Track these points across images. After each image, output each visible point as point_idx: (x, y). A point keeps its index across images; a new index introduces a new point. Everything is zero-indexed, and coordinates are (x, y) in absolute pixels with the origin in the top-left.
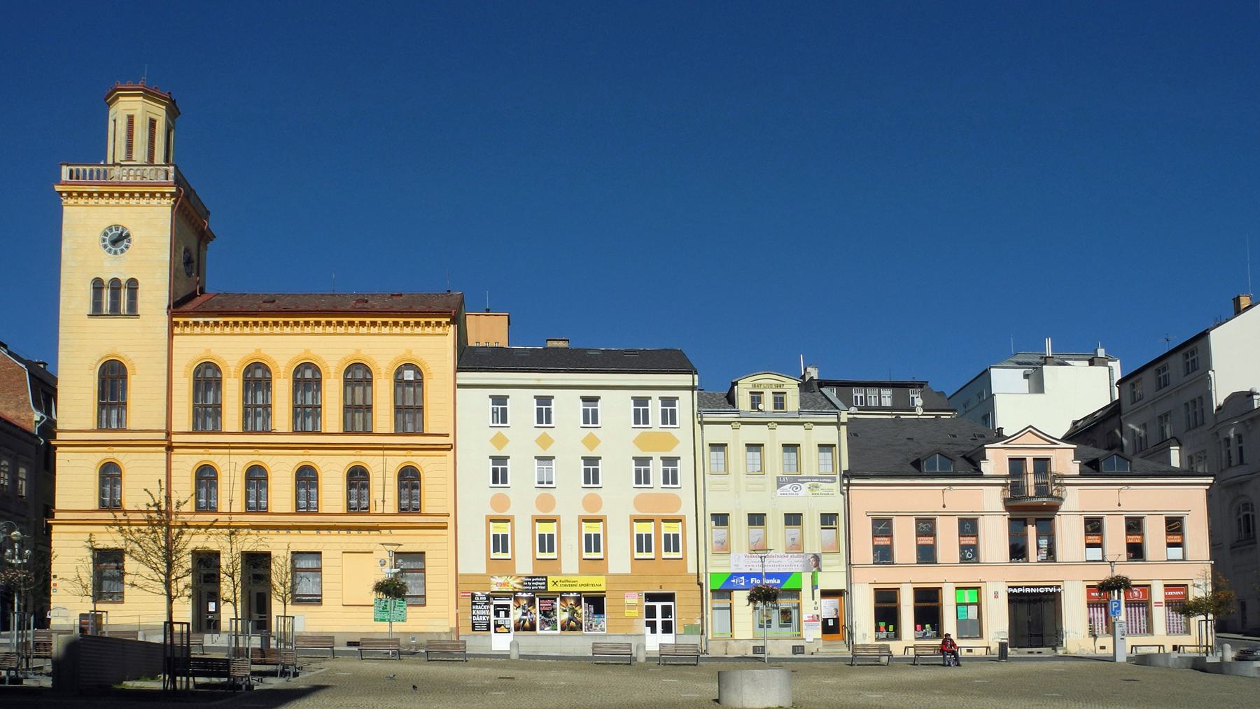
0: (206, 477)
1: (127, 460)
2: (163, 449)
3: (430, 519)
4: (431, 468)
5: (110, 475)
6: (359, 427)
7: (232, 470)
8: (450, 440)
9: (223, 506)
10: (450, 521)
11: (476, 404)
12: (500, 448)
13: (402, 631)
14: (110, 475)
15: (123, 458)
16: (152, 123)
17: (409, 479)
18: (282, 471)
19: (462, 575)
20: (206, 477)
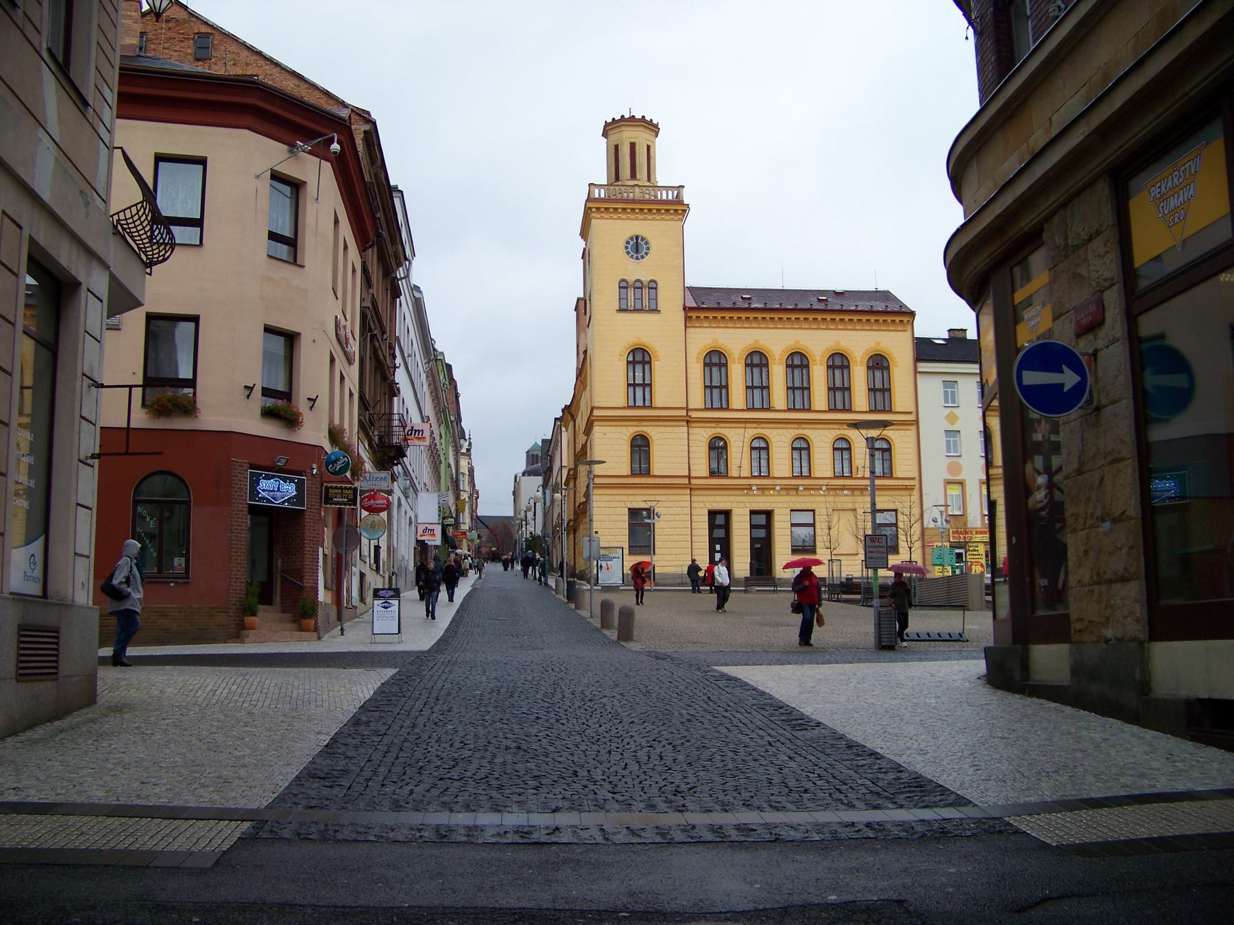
0: (718, 448)
1: (656, 434)
2: (685, 423)
3: (901, 482)
4: (901, 440)
5: (641, 446)
6: (839, 406)
7: (738, 441)
8: (912, 417)
10: (915, 483)
11: (931, 388)
12: (952, 424)
14: (641, 446)
16: (633, 146)
18: (781, 441)
19: (927, 528)
20: (718, 448)
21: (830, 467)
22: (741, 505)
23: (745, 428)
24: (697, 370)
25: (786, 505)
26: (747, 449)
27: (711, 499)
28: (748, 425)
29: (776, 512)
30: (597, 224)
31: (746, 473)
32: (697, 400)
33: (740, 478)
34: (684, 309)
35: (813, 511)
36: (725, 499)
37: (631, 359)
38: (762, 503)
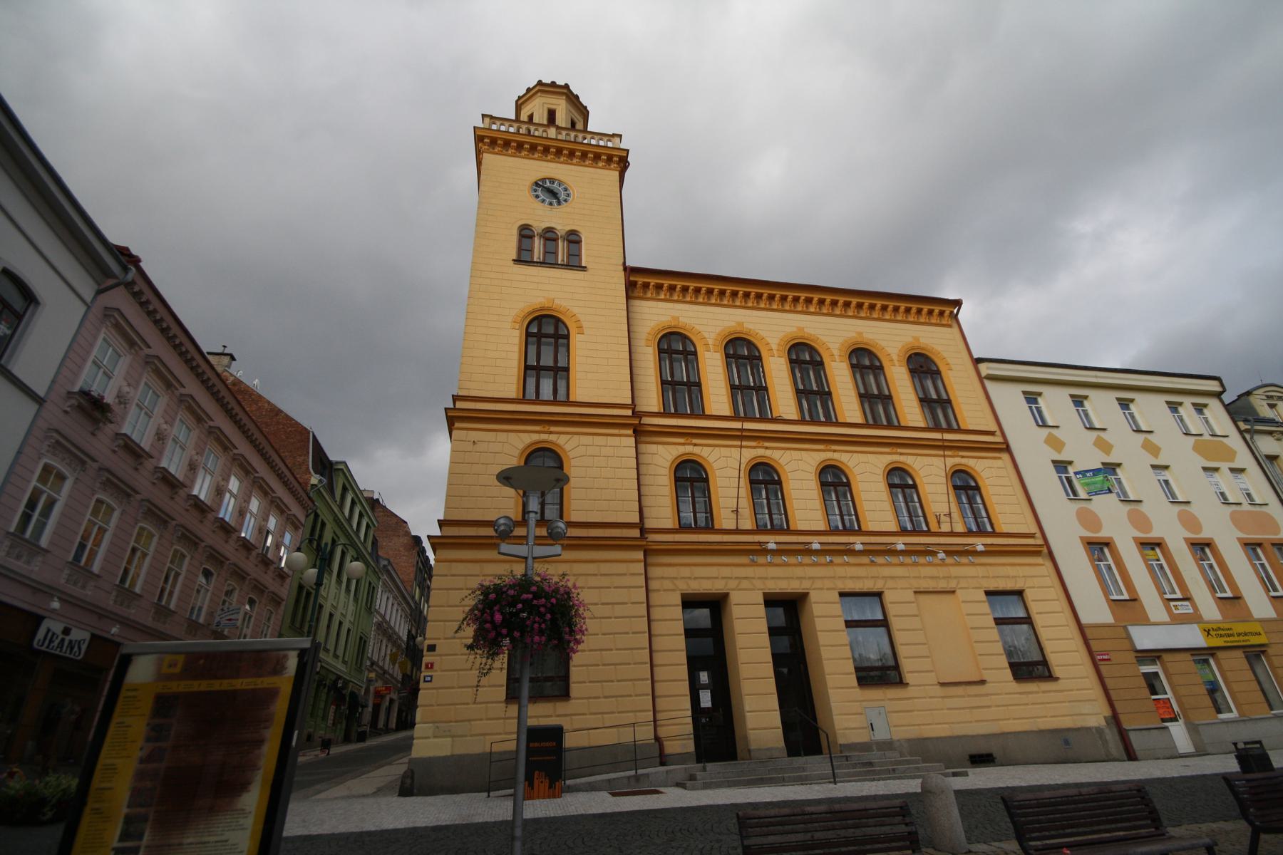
2: (630, 432)
9: (725, 519)
13: (1043, 727)
15: (574, 446)
17: (965, 485)
21: (890, 515)
22: (745, 584)
23: (741, 447)
24: (648, 358)
25: (828, 584)
26: (744, 483)
27: (685, 572)
28: (744, 443)
29: (814, 596)
30: (487, 157)
31: (747, 524)
32: (651, 399)
33: (737, 531)
34: (625, 268)
35: (879, 595)
36: (713, 571)
37: (534, 330)
38: (786, 579)
